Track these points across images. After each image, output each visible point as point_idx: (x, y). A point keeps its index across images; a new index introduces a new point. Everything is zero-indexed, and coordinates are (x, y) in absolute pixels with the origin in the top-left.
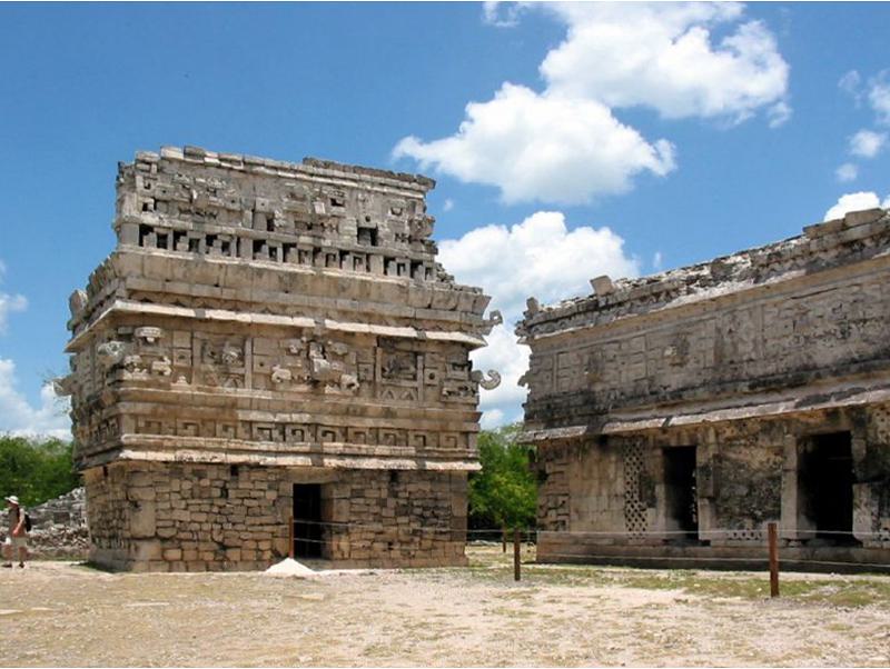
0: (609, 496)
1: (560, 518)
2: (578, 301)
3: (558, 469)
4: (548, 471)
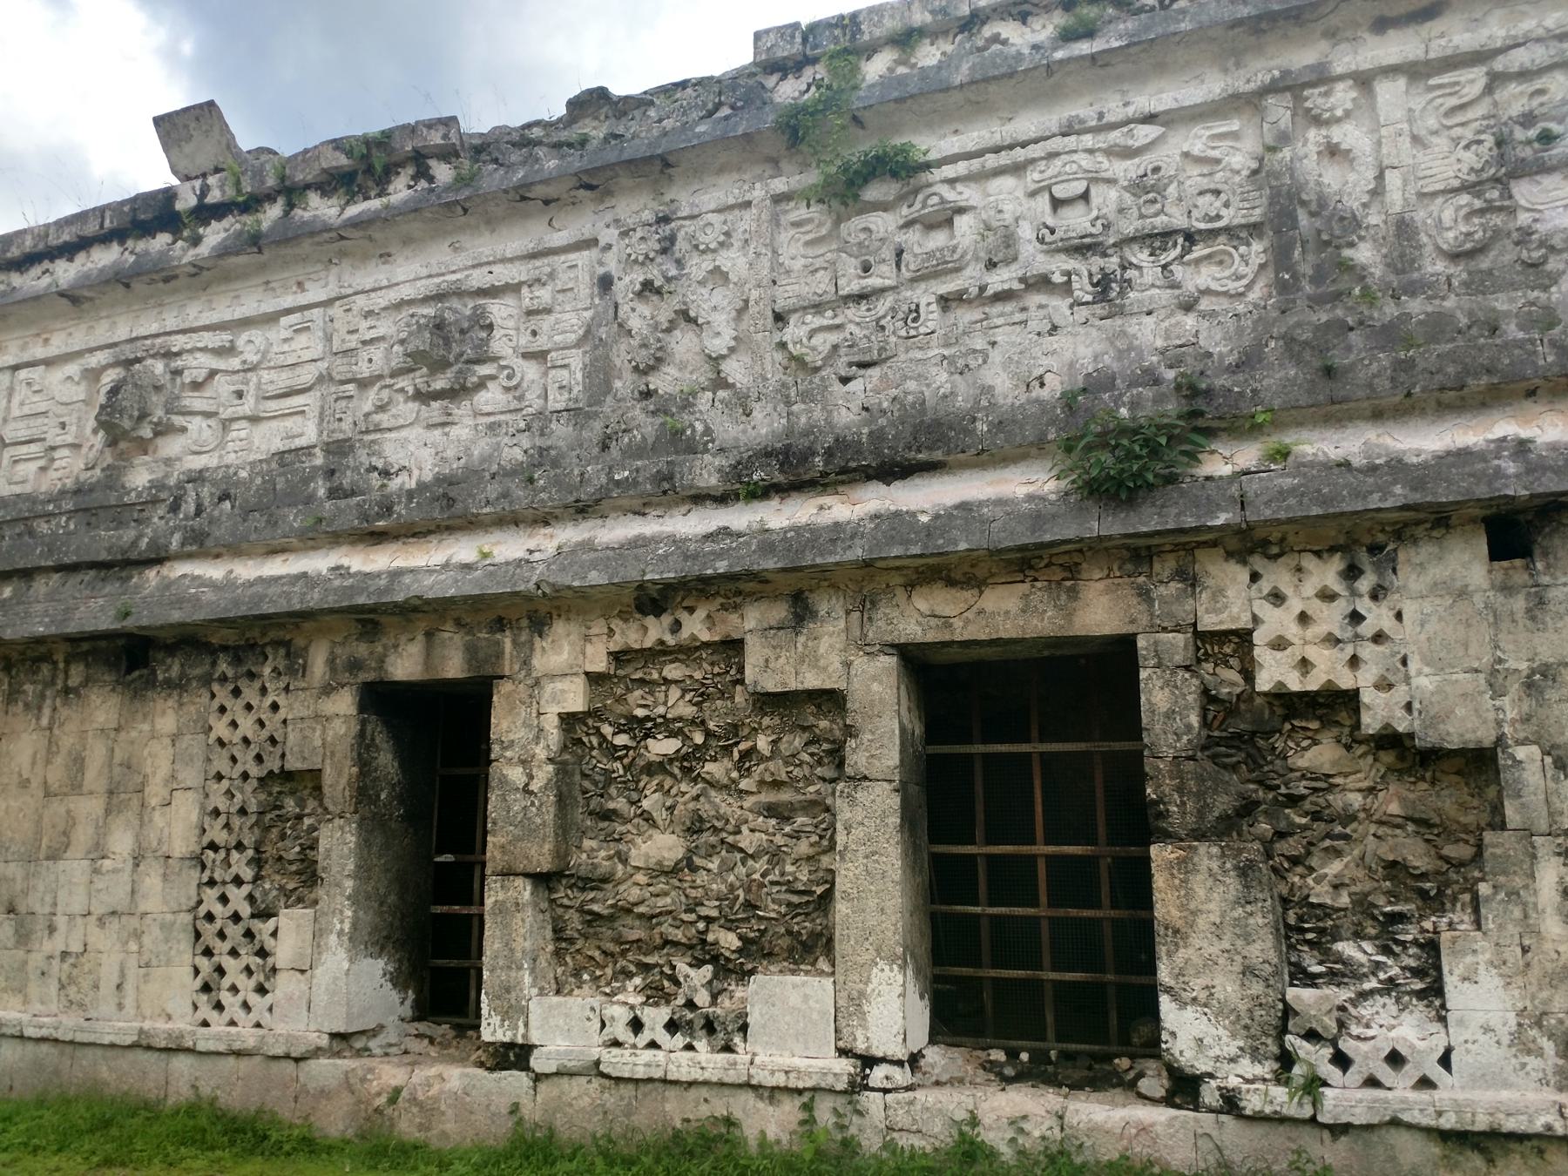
0: (137, 860)
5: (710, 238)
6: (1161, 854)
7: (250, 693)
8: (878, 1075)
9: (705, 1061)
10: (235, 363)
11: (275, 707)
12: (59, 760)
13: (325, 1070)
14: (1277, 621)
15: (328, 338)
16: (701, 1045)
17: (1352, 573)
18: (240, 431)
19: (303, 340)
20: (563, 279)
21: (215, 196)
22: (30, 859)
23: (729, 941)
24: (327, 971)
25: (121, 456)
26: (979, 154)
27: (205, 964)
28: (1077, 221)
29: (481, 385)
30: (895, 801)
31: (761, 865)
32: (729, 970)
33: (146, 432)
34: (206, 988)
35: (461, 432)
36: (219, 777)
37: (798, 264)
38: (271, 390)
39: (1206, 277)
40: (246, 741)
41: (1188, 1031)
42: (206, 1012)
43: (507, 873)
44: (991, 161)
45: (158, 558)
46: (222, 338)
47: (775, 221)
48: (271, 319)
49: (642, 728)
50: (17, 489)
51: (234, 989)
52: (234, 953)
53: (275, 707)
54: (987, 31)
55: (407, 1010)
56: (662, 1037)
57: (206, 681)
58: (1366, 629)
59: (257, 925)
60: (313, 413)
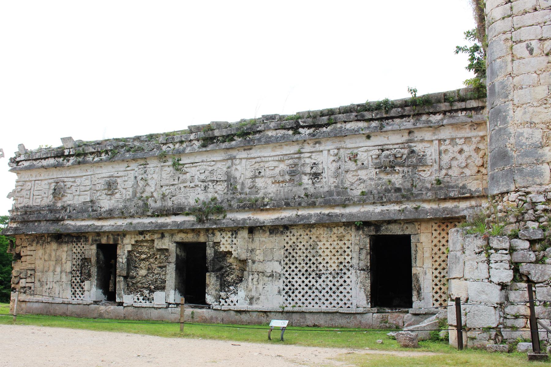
1: (28, 285)
2: (49, 150)
3: (29, 253)
4: (22, 254)
5: (152, 172)
6: (208, 274)
7: (79, 245)
8: (170, 306)
9: (148, 304)
10: (75, 184)
11: (83, 247)
12: (47, 255)
13: (93, 306)
14: (223, 241)
15: (91, 181)
16: (147, 302)
17: (232, 235)
18: (76, 197)
19: (87, 181)
20: (129, 176)
21: (71, 153)
22: (42, 272)
23: (153, 287)
24: (92, 291)
25: (56, 200)
27: (73, 290)
29: (116, 193)
30: (175, 266)
31: (158, 276)
32: (152, 291)
33: (60, 196)
34: (73, 294)
35: (113, 201)
36: (74, 259)
37: (165, 178)
38: (82, 190)
40: (79, 253)
41: (209, 299)
42: (73, 298)
43: (120, 276)
45: (63, 219)
46: (73, 180)
47: (162, 170)
49: (141, 253)
50: (37, 204)
51: (78, 294)
52: (78, 288)
53: (83, 247)
55: (106, 299)
56: (142, 301)
57: (72, 242)
58: (233, 243)
59: (81, 283)
60: (89, 195)
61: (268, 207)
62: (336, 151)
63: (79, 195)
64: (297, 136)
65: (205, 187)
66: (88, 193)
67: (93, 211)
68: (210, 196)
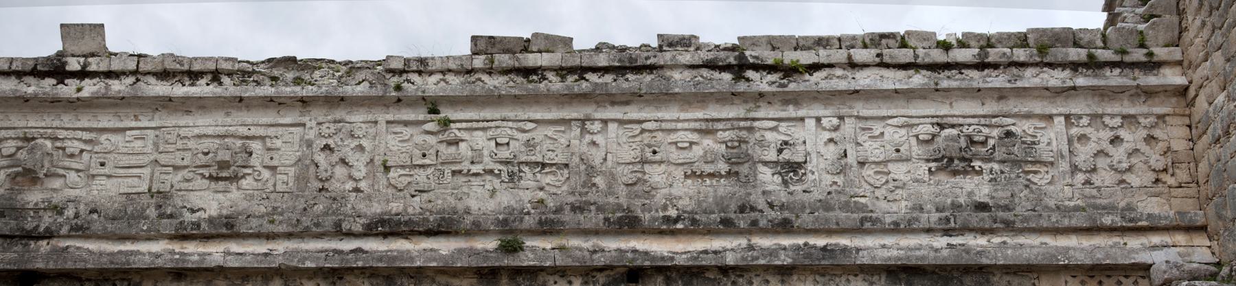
19: (139, 143)
26: (471, 121)
28: (504, 154)
29: (243, 177)
38: (121, 164)
39: (549, 179)
44: (475, 125)
45: (49, 235)
48: (123, 130)
54: (477, 76)
61: (680, 226)
62: (835, 121)
63: (109, 176)
64: (742, 87)
65: (511, 175)
66: (146, 172)
67: (161, 216)
68: (526, 196)
